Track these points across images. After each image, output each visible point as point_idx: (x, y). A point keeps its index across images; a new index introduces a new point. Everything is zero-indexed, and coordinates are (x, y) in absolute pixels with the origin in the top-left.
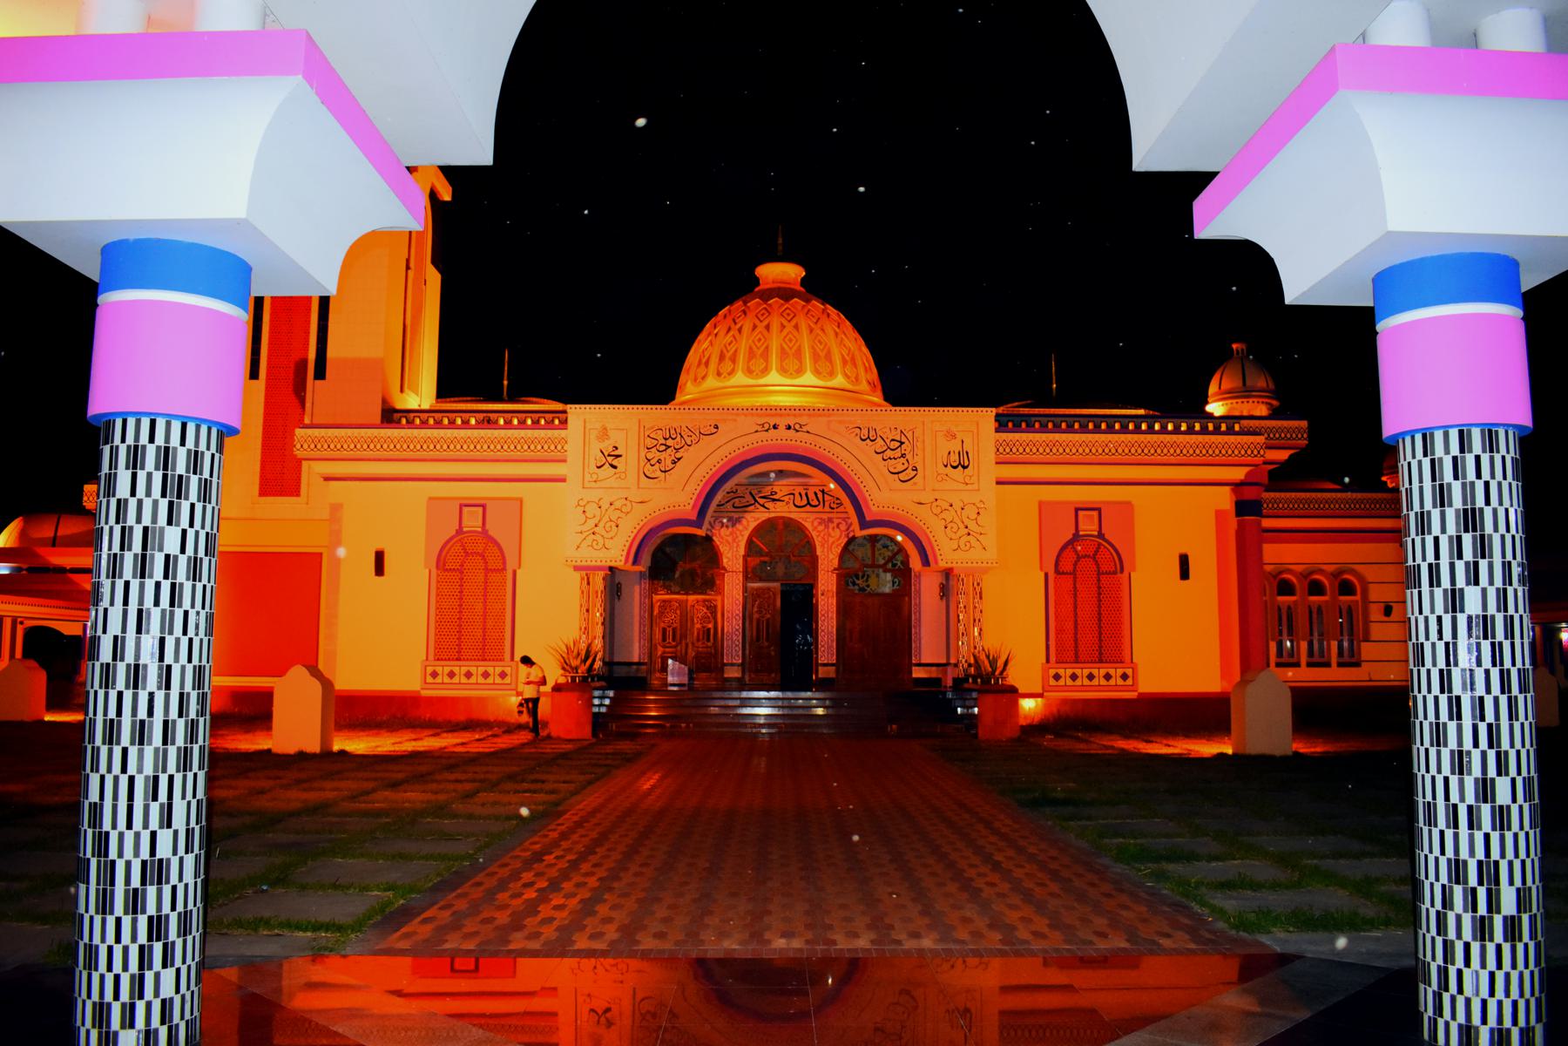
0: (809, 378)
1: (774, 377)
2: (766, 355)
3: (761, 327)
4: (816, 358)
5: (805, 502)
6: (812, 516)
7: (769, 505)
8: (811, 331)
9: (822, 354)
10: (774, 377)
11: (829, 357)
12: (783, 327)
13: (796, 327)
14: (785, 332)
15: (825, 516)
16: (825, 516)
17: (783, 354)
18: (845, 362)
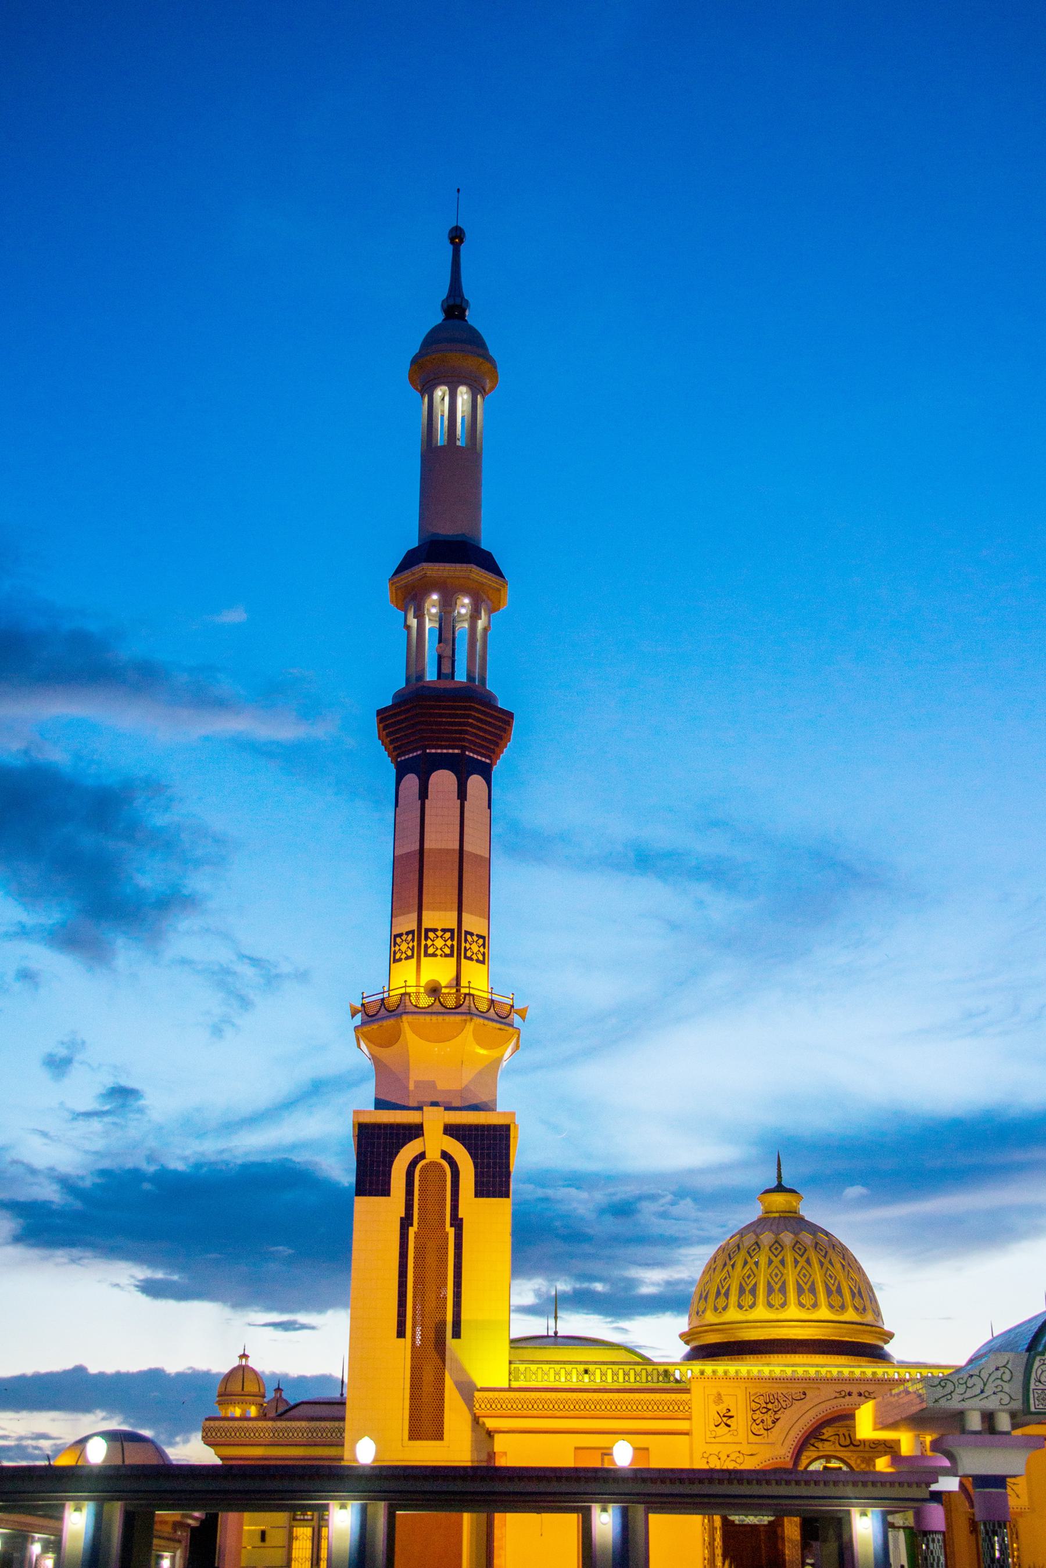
0: (824, 1313)
1: (793, 1312)
2: (783, 1290)
3: (776, 1261)
4: (829, 1292)
5: (848, 1442)
6: (855, 1455)
7: (819, 1445)
8: (822, 1264)
9: (834, 1289)
10: (793, 1312)
11: (839, 1291)
12: (796, 1262)
13: (808, 1261)
14: (799, 1268)
15: (866, 1455)
16: (866, 1455)
17: (800, 1291)
18: (853, 1295)
